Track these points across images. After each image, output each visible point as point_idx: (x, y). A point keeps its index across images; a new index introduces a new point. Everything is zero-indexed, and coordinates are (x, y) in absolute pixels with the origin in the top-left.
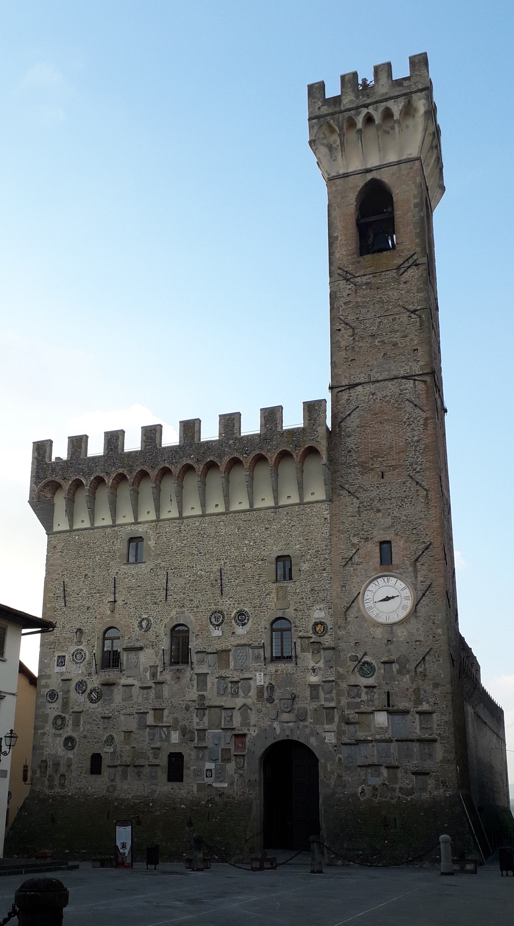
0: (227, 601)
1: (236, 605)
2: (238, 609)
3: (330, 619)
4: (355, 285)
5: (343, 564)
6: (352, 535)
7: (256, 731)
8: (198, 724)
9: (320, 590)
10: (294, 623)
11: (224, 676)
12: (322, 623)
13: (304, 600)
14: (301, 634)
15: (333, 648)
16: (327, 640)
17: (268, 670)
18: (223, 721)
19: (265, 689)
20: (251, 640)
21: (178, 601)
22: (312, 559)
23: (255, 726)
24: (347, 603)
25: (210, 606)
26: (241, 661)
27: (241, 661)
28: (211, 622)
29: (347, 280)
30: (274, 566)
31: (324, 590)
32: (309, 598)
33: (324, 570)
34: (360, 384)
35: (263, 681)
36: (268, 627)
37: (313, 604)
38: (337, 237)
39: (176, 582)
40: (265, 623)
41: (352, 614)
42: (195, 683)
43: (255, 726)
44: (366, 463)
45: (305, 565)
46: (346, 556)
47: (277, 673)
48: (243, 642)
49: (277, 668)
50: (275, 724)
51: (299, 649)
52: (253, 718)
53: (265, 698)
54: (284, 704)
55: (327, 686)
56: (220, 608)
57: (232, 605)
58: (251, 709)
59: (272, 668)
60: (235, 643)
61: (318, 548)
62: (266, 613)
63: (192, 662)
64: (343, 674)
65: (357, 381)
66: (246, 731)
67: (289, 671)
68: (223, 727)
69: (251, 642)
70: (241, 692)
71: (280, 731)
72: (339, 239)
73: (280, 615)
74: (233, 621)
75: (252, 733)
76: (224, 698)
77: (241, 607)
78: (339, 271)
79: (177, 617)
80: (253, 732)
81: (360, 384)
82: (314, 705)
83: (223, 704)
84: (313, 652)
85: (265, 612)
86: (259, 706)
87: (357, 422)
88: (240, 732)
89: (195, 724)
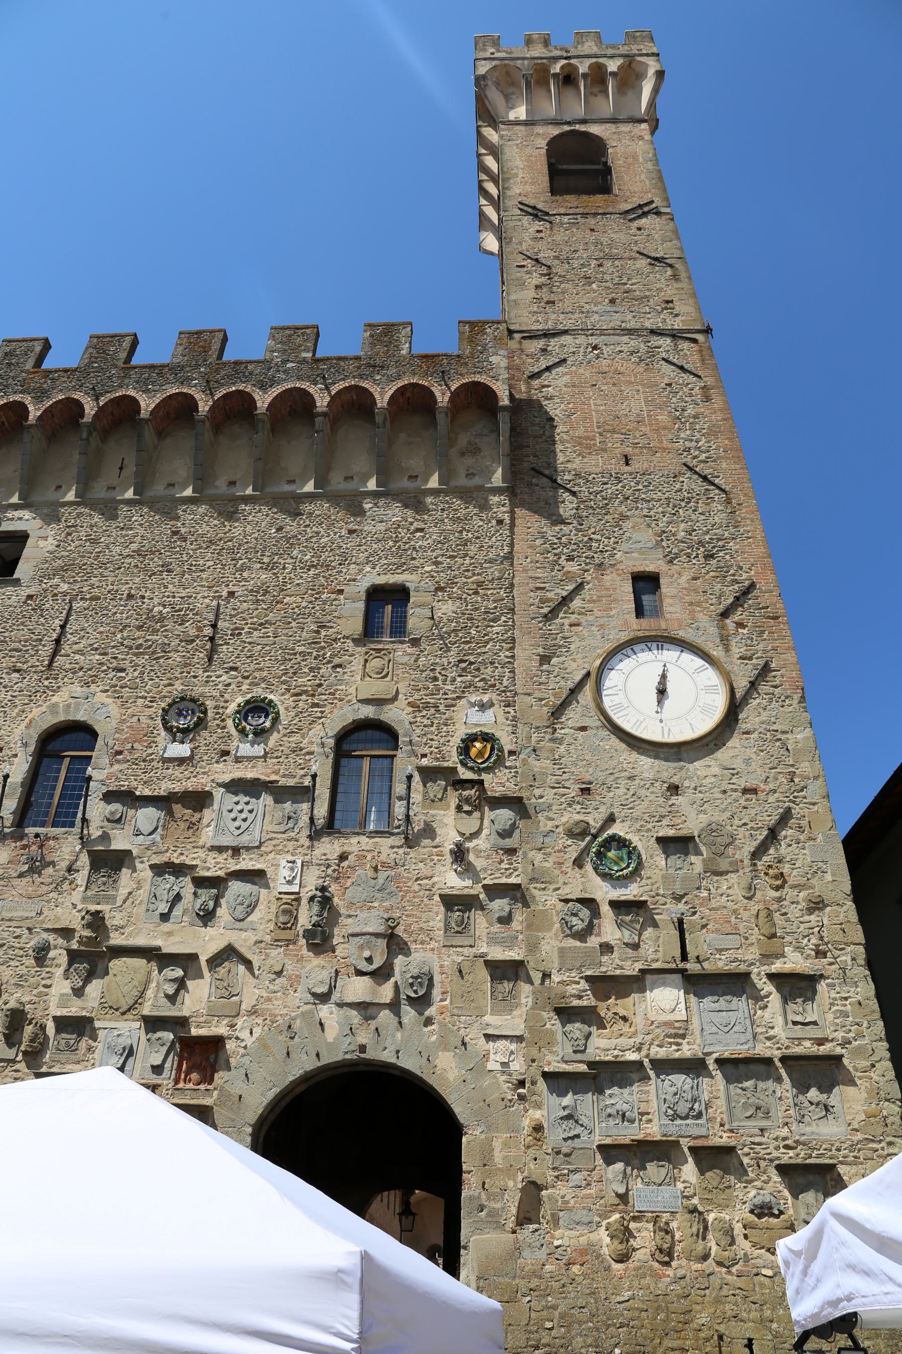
0: (220, 676)
1: (245, 687)
2: (249, 696)
3: (510, 729)
4: (551, 223)
5: (545, 610)
6: (563, 557)
7: (257, 1031)
8: (63, 1001)
9: (483, 663)
10: (405, 736)
11: (177, 861)
12: (487, 738)
13: (440, 683)
14: (425, 762)
15: (516, 803)
16: (497, 783)
17: (317, 852)
18: (150, 993)
19: (304, 901)
20: (276, 772)
21: (81, 669)
22: (465, 596)
23: (253, 1012)
24: (555, 695)
25: (170, 685)
26: (237, 824)
27: (237, 824)
28: (165, 722)
29: (536, 216)
30: (361, 605)
31: (492, 663)
32: (454, 680)
33: (495, 620)
34: (566, 332)
35: (297, 881)
36: (331, 742)
37: (463, 692)
38: (516, 175)
39: (85, 634)
40: (321, 735)
41: (573, 716)
42: (81, 878)
43: (253, 1012)
44: (587, 438)
45: (446, 607)
46: (550, 595)
47: (345, 864)
48: (250, 775)
49: (346, 848)
50: (325, 1011)
51: (416, 797)
52: (250, 991)
53: (300, 929)
54: (361, 948)
55: (500, 905)
56: (197, 691)
57: (233, 686)
58: (248, 963)
59: (330, 848)
60: (227, 778)
61: (478, 574)
62: (327, 709)
63: (84, 820)
64: (546, 871)
65: (560, 327)
66: (221, 1030)
67: (383, 857)
68: (146, 1012)
69: (273, 777)
70: (223, 912)
71: (336, 1037)
72: (520, 176)
73: (368, 711)
74: (230, 723)
75: (244, 1035)
76: (167, 927)
77: (259, 692)
78: (520, 206)
79: (69, 706)
80: (244, 1038)
81: (566, 332)
82: (455, 957)
83: (158, 942)
84: (459, 808)
85: (325, 706)
86: (277, 955)
87: (566, 379)
88: (203, 1032)
89: (53, 1002)
